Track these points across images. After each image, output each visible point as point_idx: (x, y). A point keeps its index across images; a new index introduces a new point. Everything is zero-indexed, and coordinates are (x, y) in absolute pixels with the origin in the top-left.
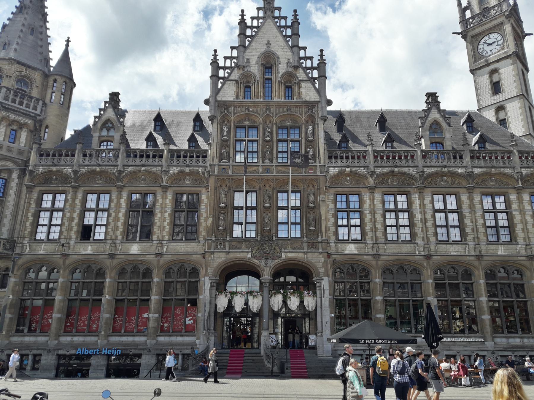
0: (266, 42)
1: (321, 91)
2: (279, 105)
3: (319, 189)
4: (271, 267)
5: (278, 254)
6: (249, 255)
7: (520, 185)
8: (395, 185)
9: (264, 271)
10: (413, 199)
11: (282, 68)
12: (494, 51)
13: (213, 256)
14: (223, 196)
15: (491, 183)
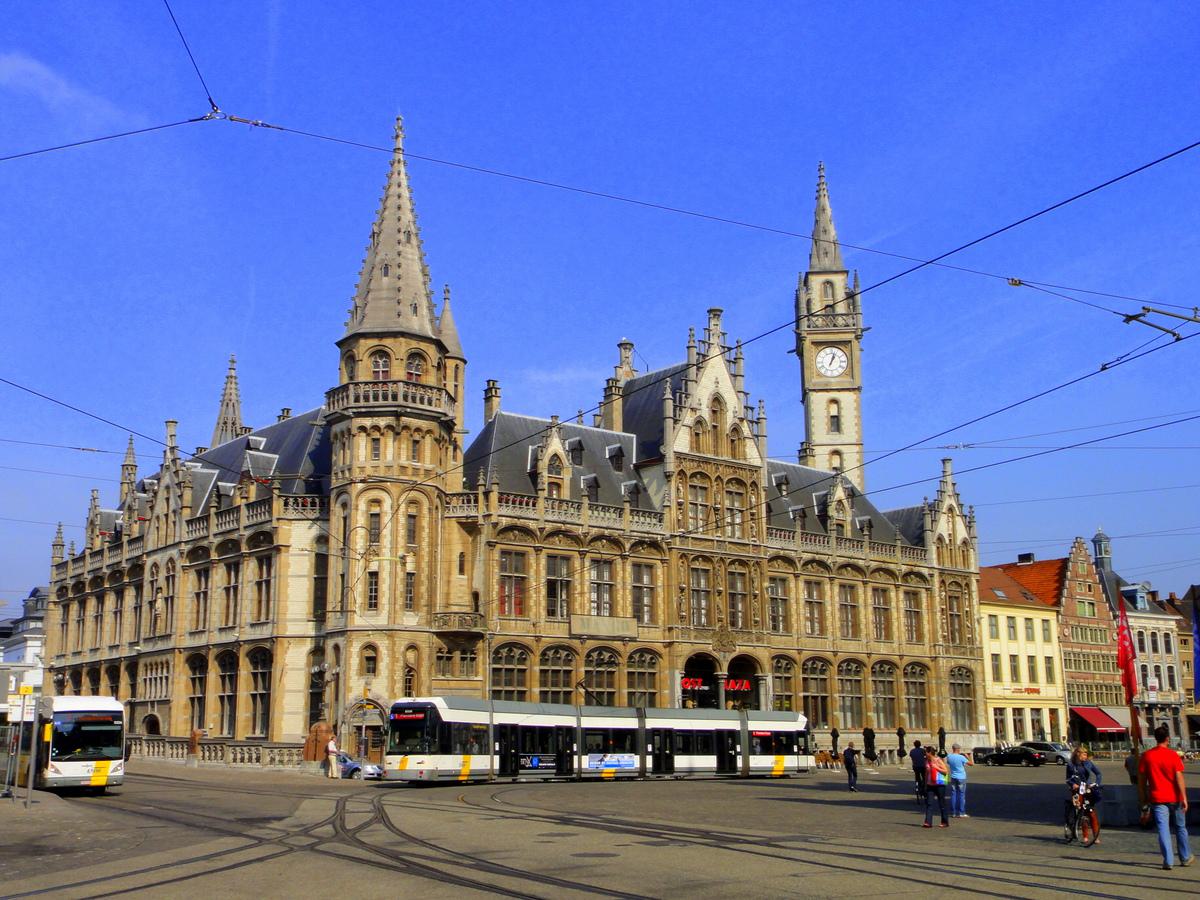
0: (714, 380)
6: (710, 648)
11: (729, 419)
12: (836, 373)
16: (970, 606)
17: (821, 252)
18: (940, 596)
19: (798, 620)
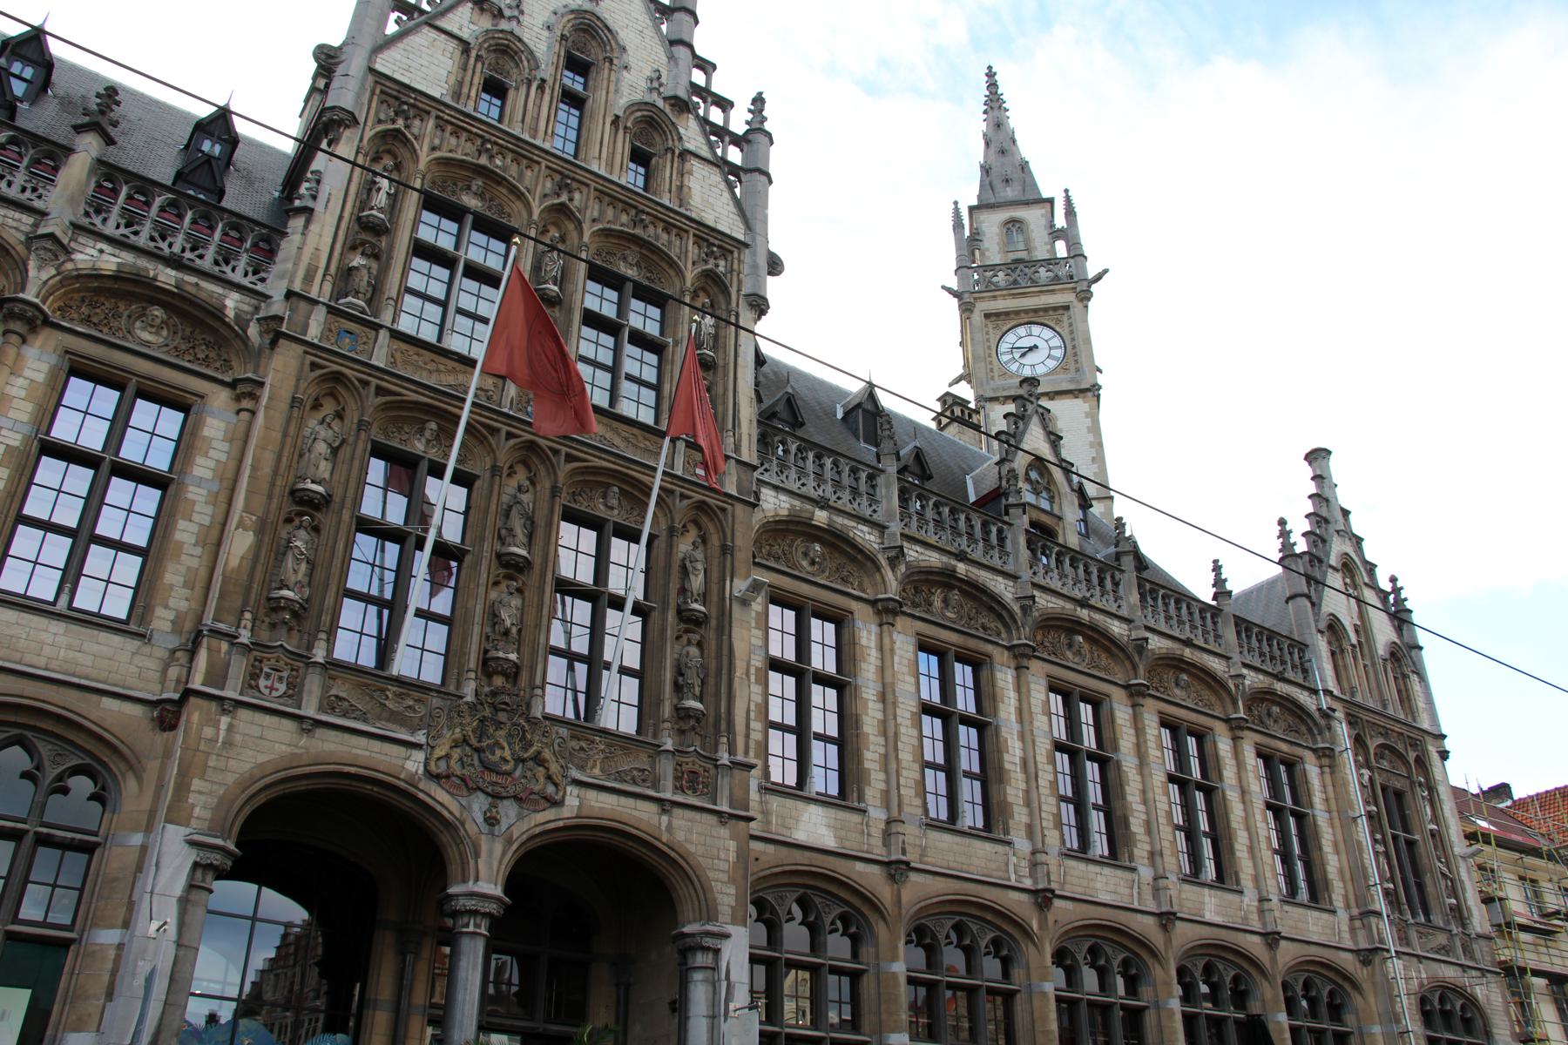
1: (750, 212)
2: (610, 194)
3: (726, 550)
4: (510, 842)
5: (551, 789)
7: (1242, 715)
8: (950, 620)
9: (477, 855)
10: (1000, 683)
13: (230, 727)
14: (321, 448)
15: (1177, 691)
16: (1436, 818)
17: (998, 184)
18: (1361, 775)
19: (889, 759)
